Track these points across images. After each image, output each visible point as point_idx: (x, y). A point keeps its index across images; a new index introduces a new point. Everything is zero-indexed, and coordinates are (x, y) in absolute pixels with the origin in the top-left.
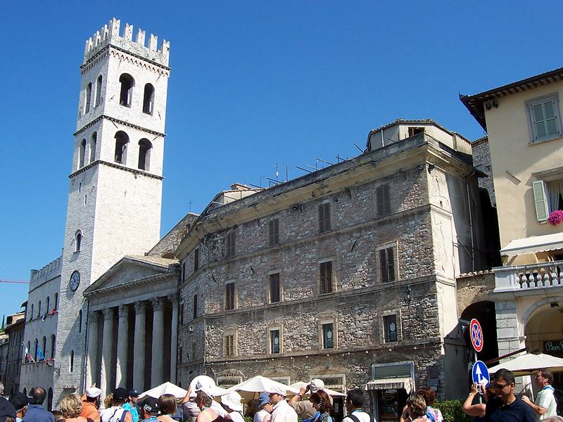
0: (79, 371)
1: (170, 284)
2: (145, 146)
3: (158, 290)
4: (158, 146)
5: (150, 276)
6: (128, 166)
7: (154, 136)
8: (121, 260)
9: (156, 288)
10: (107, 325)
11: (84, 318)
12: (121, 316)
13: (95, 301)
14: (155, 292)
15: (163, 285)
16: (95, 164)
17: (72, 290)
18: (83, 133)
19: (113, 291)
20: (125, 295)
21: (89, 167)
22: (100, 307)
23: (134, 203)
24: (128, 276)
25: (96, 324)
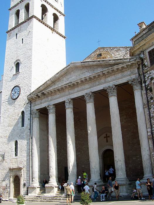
0: (25, 154)
2: (56, 18)
3: (114, 80)
4: (62, 19)
5: (99, 70)
10: (52, 118)
11: (27, 116)
12: (69, 108)
15: (120, 75)
16: (29, 19)
17: (13, 99)
19: (61, 90)
20: (71, 91)
21: (22, 23)
22: (43, 106)
24: (73, 77)
25: (38, 119)
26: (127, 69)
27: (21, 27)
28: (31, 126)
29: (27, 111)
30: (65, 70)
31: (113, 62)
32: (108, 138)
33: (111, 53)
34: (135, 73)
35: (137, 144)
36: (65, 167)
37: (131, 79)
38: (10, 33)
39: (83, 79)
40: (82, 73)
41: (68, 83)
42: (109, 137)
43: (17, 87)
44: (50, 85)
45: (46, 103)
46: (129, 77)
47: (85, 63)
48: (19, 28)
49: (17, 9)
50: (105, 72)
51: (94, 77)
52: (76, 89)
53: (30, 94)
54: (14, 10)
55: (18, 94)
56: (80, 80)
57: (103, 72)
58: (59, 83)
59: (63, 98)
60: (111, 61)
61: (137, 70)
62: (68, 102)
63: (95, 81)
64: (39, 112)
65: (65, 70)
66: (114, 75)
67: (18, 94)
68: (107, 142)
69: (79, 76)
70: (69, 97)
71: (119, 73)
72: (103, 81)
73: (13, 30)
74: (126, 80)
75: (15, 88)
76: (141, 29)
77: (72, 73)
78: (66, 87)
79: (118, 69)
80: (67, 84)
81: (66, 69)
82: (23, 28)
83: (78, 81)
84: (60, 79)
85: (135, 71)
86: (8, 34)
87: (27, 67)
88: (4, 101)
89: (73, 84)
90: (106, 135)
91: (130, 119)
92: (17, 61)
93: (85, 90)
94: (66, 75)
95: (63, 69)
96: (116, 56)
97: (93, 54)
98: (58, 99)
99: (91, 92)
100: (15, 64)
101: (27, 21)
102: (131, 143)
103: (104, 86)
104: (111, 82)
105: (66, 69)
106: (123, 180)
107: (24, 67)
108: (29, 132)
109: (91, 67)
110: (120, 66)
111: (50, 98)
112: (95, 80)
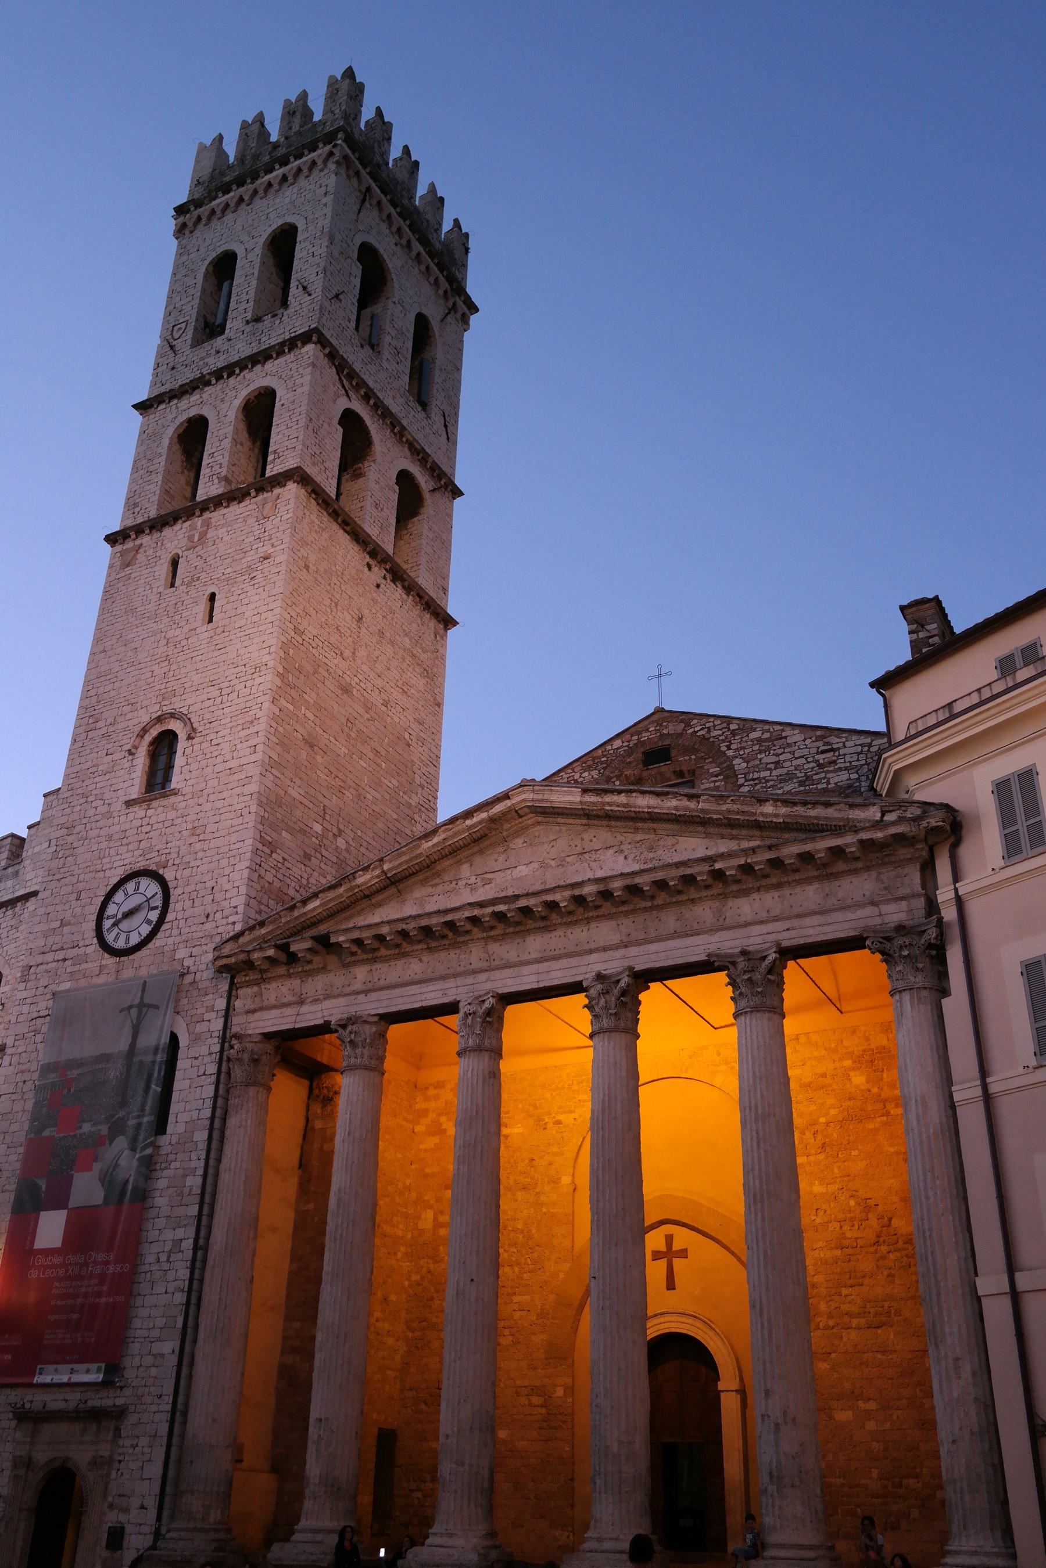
1: (859, 886)
3: (776, 919)
6: (372, 530)
7: (431, 485)
8: (505, 796)
9: (745, 907)
13: (279, 989)
14: (747, 924)
15: (809, 895)
18: (195, 398)
22: (311, 1016)
23: (379, 667)
24: (523, 870)
26: (860, 865)
27: (207, 525)
28: (216, 1135)
29: (196, 1039)
30: (475, 820)
31: (777, 816)
32: (677, 1263)
33: (730, 753)
34: (908, 891)
35: (862, 1321)
36: (380, 1429)
37: (878, 921)
38: (129, 545)
39: (587, 890)
40: (579, 849)
41: (494, 902)
42: (683, 1253)
43: (144, 882)
44: (367, 897)
45: (327, 1004)
46: (870, 910)
47: (608, 798)
48: (193, 528)
49: (193, 412)
50: (730, 868)
51: (661, 885)
52: (536, 944)
53: (236, 937)
54: (170, 417)
55: (149, 922)
56: (567, 894)
57: (718, 866)
58: (429, 890)
59: (450, 983)
60: (768, 808)
61: (918, 873)
62: (481, 1011)
63: (659, 908)
64: (277, 1048)
65: (475, 820)
66: (778, 886)
67: (149, 922)
68: (671, 1285)
69: (563, 866)
70: (488, 986)
71: (808, 881)
72: (704, 912)
73: (156, 535)
74: (846, 925)
75: (130, 886)
76: (921, 635)
77: (519, 842)
78: (475, 920)
79: (806, 858)
80: (481, 905)
81: (484, 815)
82: (222, 532)
83: (557, 897)
84: (439, 868)
85: (906, 880)
86: (119, 548)
87: (233, 764)
88: (39, 959)
89: (526, 911)
90: (669, 1239)
91: (821, 1157)
92: (159, 719)
93: (591, 952)
94: (481, 852)
95: (468, 814)
96: (756, 775)
97: (617, 743)
98: (414, 989)
99: (630, 969)
100: (148, 738)
101: (253, 494)
102: (823, 1306)
103: (713, 948)
104: (757, 929)
105: (484, 815)
106: (812, 1554)
107: (204, 763)
108: (200, 1172)
109: (640, 825)
110: (821, 845)
111: (361, 974)
112: (659, 901)
